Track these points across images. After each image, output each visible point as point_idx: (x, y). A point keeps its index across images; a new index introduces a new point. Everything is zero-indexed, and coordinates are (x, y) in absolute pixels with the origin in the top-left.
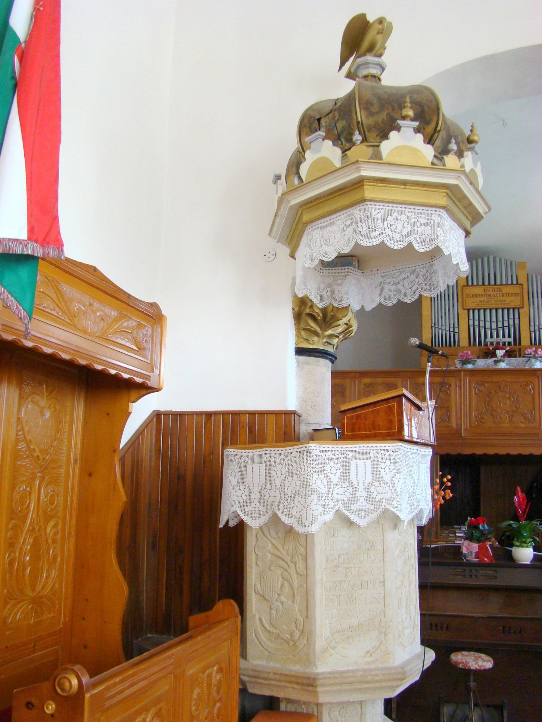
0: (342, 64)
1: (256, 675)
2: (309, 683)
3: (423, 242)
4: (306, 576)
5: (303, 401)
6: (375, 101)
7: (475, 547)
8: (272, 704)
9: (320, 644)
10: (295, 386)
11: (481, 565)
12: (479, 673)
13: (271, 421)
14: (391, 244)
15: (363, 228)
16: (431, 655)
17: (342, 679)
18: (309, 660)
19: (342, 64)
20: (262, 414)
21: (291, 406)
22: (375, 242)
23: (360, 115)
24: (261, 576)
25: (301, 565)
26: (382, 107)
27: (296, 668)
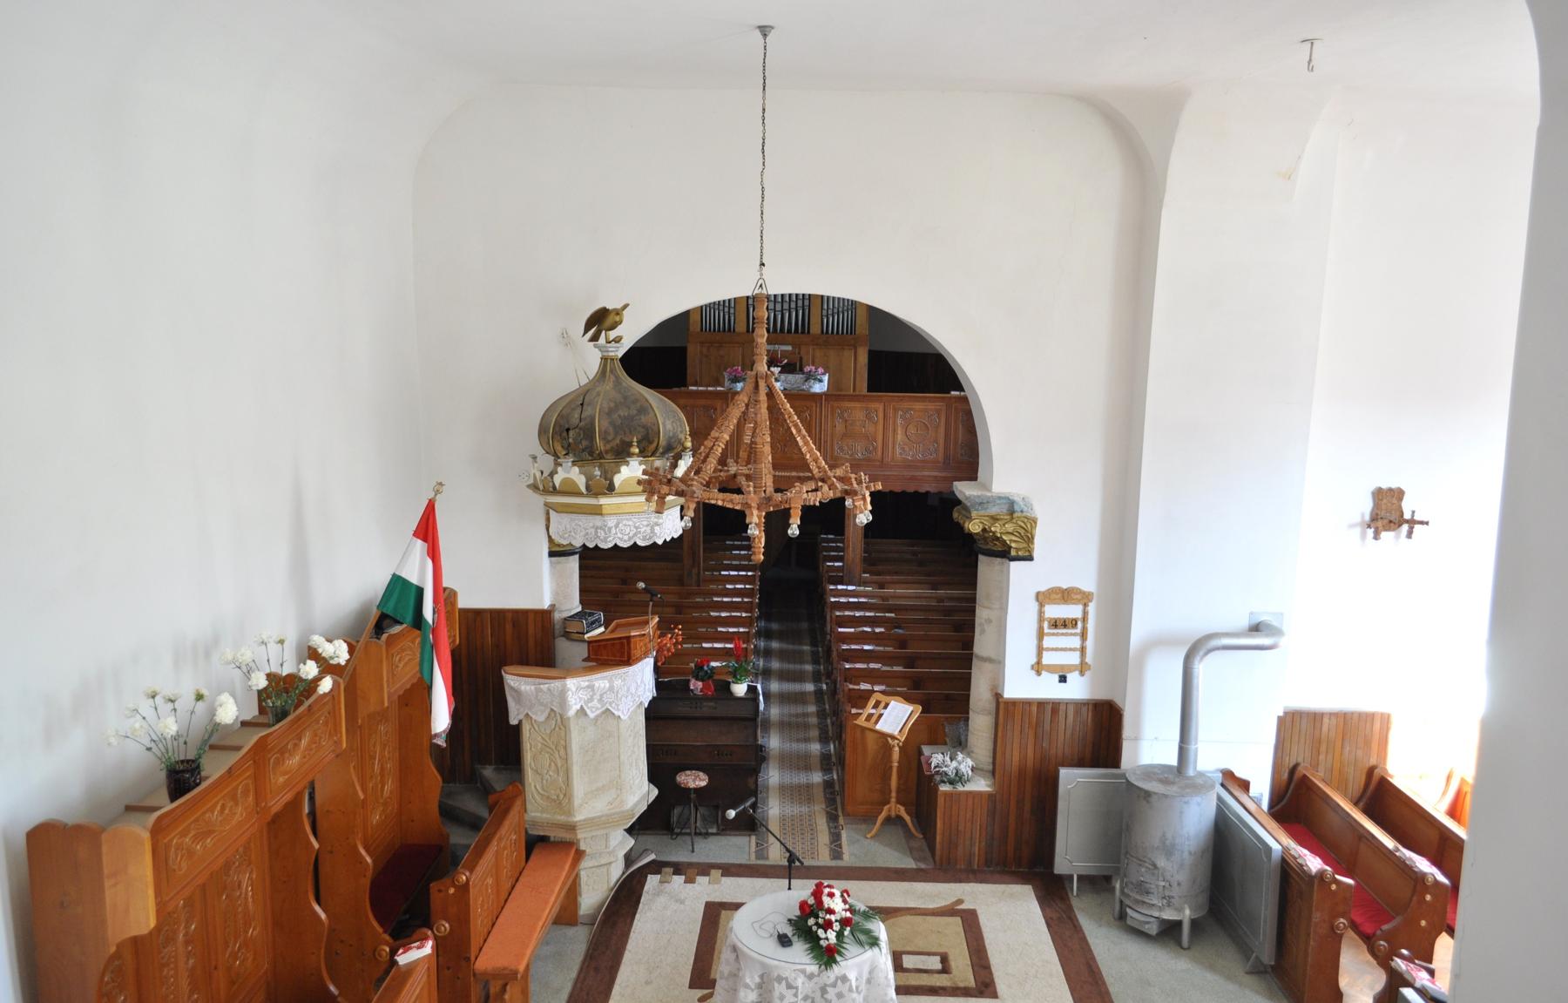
0: (586, 331)
1: (534, 823)
2: (572, 828)
3: (644, 539)
4: (566, 760)
5: (556, 594)
6: (611, 430)
7: (700, 684)
8: (543, 839)
9: (577, 802)
10: (549, 588)
11: (705, 698)
12: (698, 790)
13: (531, 617)
14: (621, 544)
15: (601, 534)
16: (655, 792)
17: (592, 823)
18: (570, 813)
19: (586, 331)
20: (525, 612)
21: (546, 605)
22: (610, 545)
23: (599, 444)
24: (534, 758)
25: (562, 752)
26: (616, 433)
27: (562, 818)
